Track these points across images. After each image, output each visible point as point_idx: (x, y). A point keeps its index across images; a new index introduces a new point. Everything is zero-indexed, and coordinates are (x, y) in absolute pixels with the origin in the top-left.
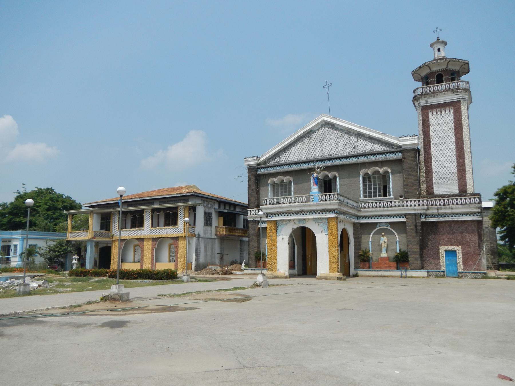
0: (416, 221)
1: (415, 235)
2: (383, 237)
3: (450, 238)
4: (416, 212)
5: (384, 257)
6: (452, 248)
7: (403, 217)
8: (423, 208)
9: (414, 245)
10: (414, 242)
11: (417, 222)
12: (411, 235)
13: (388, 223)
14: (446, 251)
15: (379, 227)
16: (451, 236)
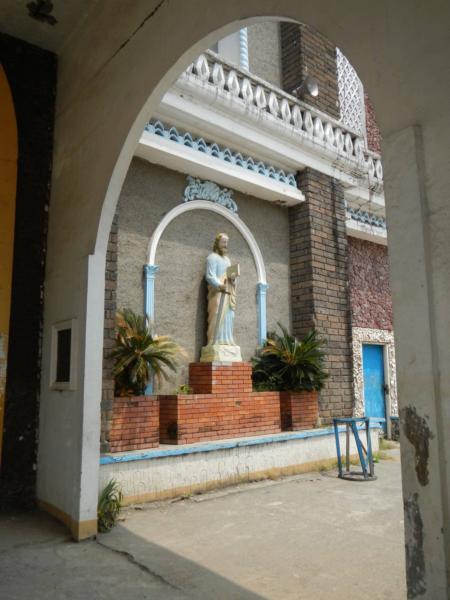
0: (334, 212)
1: (333, 269)
2: (221, 254)
3: (375, 301)
4: (336, 174)
5: (235, 365)
6: (379, 334)
7: (291, 184)
8: (359, 168)
9: (331, 312)
10: (331, 299)
11: (338, 216)
12: (321, 265)
13: (229, 194)
14: (367, 346)
15: (196, 199)
16: (376, 296)
